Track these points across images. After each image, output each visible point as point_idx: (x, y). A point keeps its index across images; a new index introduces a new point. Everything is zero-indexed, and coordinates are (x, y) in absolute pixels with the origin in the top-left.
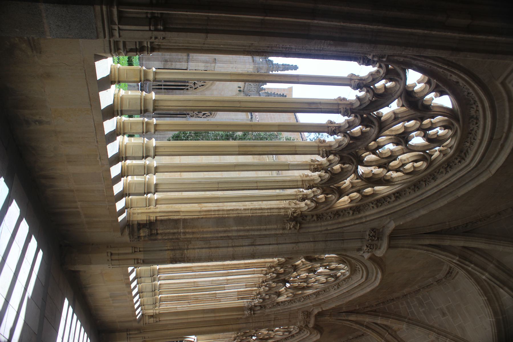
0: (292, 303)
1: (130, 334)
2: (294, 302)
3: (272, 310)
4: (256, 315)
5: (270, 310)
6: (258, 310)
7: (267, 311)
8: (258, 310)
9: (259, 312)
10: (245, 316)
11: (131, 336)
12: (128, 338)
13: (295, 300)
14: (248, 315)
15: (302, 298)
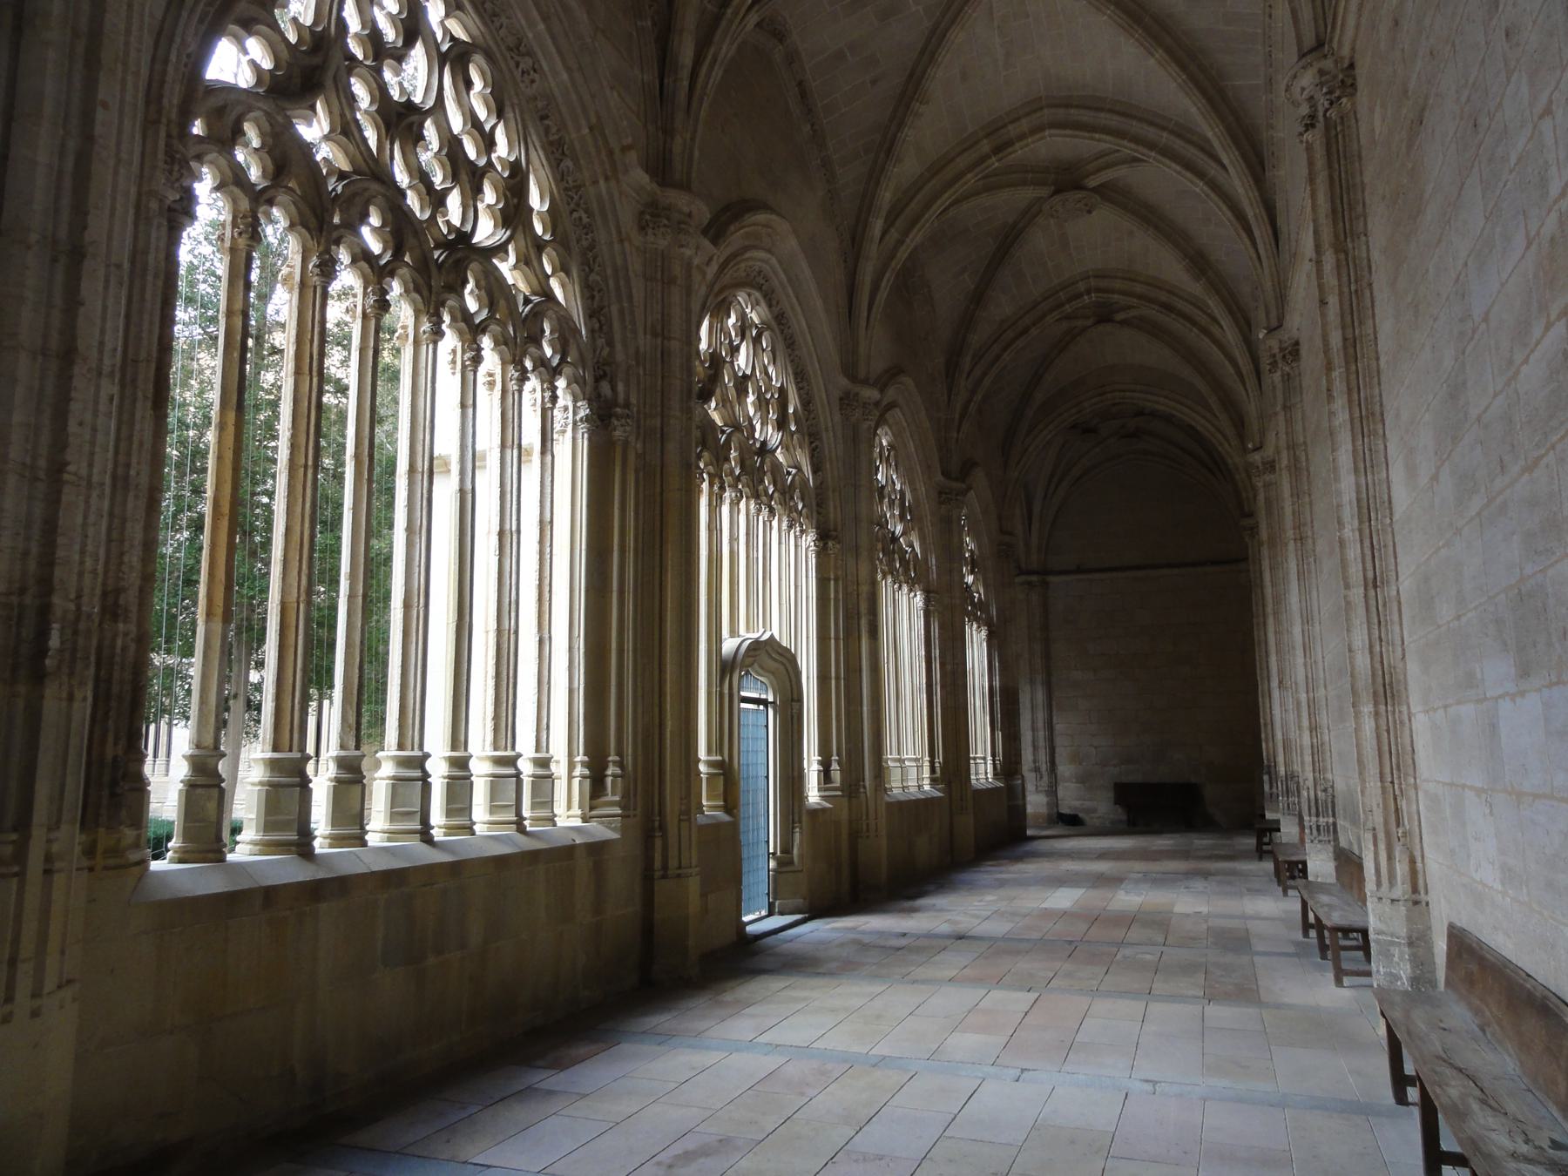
0: (595, 259)
1: (665, 867)
2: (591, 247)
3: (617, 336)
4: (633, 400)
5: (619, 347)
6: (614, 389)
7: (620, 357)
8: (614, 389)
9: (620, 387)
10: (632, 439)
11: (673, 863)
12: (679, 876)
13: (585, 243)
14: (628, 428)
15: (575, 215)
